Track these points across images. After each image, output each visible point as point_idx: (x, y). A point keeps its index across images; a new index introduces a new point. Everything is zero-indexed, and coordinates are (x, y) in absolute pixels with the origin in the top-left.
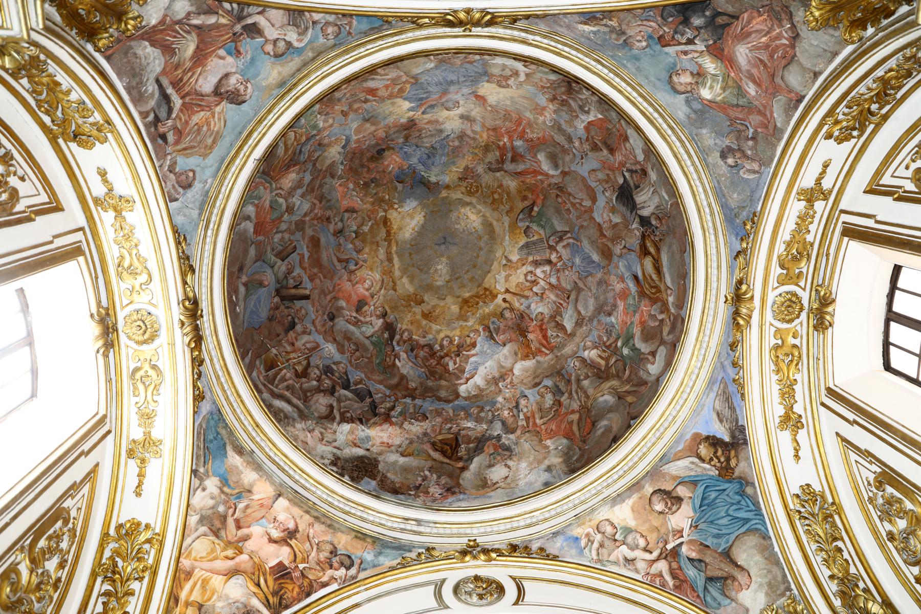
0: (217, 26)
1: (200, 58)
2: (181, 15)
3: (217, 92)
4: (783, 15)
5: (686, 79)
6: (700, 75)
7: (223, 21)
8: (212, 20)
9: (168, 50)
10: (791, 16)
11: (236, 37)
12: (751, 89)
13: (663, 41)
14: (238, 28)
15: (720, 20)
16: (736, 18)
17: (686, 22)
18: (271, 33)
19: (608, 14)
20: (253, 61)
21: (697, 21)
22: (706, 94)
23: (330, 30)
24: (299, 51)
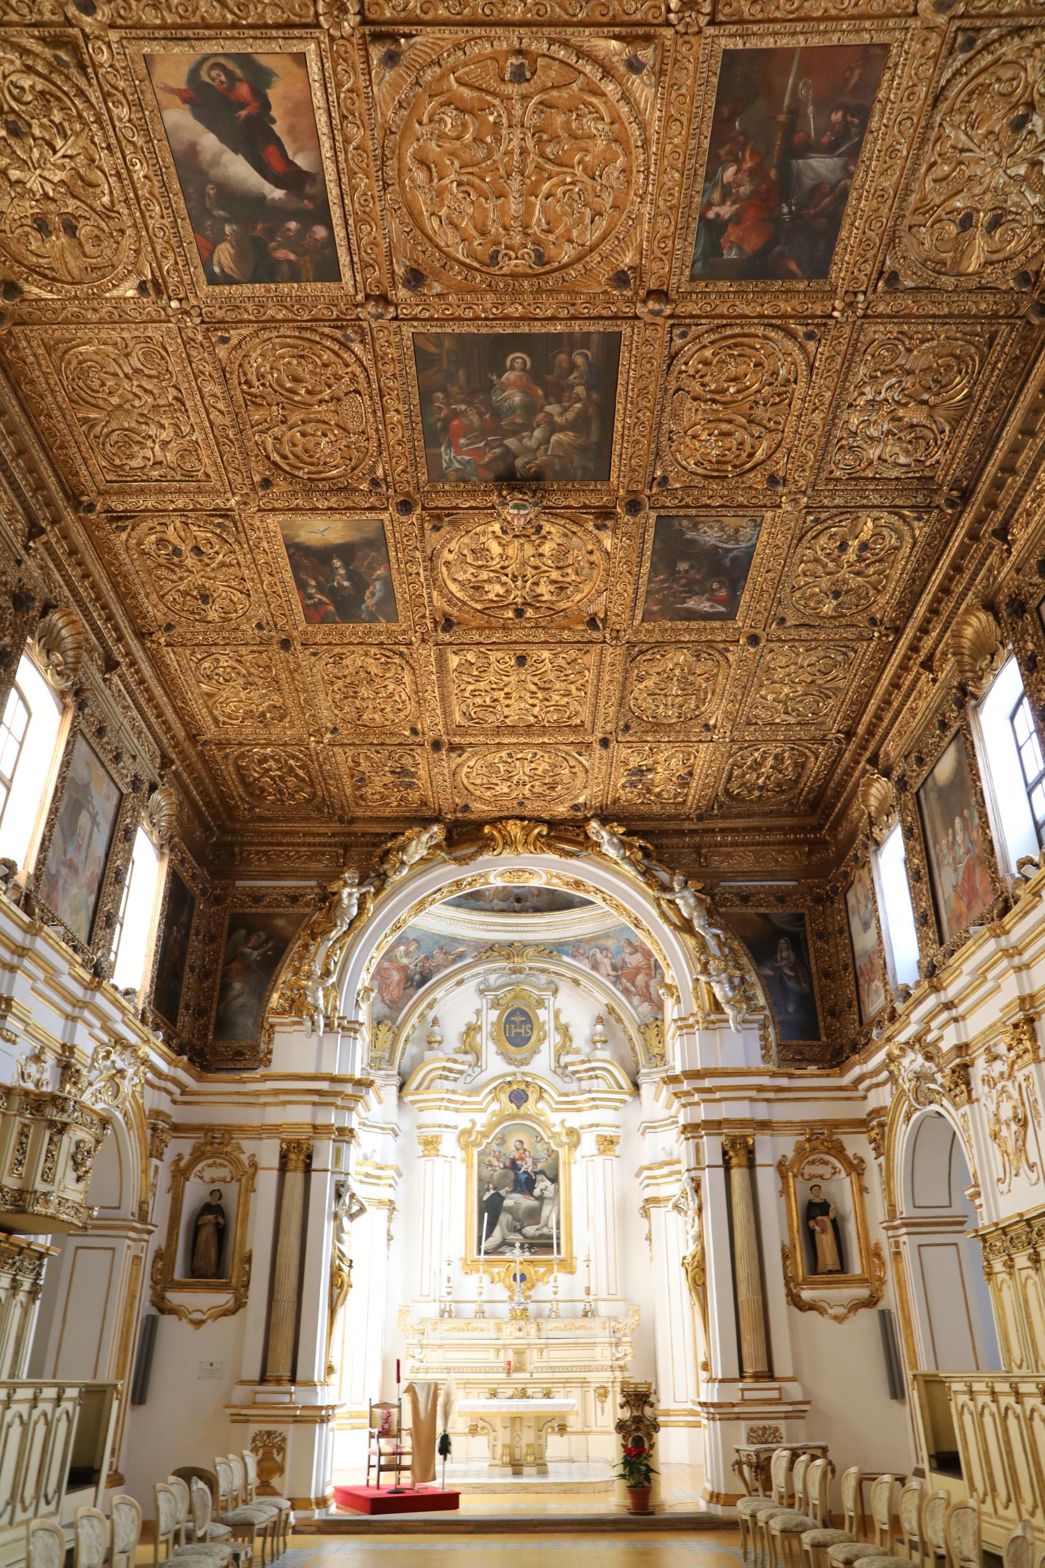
0: (629, 980)
1: (638, 970)
3: (636, 951)
5: (412, 948)
6: (407, 954)
7: (624, 980)
8: (628, 985)
9: (647, 986)
10: (390, 1008)
11: (622, 968)
12: (386, 965)
13: (427, 958)
17: (421, 973)
18: (607, 961)
19: (454, 961)
21: (417, 977)
22: (402, 948)
24: (597, 947)
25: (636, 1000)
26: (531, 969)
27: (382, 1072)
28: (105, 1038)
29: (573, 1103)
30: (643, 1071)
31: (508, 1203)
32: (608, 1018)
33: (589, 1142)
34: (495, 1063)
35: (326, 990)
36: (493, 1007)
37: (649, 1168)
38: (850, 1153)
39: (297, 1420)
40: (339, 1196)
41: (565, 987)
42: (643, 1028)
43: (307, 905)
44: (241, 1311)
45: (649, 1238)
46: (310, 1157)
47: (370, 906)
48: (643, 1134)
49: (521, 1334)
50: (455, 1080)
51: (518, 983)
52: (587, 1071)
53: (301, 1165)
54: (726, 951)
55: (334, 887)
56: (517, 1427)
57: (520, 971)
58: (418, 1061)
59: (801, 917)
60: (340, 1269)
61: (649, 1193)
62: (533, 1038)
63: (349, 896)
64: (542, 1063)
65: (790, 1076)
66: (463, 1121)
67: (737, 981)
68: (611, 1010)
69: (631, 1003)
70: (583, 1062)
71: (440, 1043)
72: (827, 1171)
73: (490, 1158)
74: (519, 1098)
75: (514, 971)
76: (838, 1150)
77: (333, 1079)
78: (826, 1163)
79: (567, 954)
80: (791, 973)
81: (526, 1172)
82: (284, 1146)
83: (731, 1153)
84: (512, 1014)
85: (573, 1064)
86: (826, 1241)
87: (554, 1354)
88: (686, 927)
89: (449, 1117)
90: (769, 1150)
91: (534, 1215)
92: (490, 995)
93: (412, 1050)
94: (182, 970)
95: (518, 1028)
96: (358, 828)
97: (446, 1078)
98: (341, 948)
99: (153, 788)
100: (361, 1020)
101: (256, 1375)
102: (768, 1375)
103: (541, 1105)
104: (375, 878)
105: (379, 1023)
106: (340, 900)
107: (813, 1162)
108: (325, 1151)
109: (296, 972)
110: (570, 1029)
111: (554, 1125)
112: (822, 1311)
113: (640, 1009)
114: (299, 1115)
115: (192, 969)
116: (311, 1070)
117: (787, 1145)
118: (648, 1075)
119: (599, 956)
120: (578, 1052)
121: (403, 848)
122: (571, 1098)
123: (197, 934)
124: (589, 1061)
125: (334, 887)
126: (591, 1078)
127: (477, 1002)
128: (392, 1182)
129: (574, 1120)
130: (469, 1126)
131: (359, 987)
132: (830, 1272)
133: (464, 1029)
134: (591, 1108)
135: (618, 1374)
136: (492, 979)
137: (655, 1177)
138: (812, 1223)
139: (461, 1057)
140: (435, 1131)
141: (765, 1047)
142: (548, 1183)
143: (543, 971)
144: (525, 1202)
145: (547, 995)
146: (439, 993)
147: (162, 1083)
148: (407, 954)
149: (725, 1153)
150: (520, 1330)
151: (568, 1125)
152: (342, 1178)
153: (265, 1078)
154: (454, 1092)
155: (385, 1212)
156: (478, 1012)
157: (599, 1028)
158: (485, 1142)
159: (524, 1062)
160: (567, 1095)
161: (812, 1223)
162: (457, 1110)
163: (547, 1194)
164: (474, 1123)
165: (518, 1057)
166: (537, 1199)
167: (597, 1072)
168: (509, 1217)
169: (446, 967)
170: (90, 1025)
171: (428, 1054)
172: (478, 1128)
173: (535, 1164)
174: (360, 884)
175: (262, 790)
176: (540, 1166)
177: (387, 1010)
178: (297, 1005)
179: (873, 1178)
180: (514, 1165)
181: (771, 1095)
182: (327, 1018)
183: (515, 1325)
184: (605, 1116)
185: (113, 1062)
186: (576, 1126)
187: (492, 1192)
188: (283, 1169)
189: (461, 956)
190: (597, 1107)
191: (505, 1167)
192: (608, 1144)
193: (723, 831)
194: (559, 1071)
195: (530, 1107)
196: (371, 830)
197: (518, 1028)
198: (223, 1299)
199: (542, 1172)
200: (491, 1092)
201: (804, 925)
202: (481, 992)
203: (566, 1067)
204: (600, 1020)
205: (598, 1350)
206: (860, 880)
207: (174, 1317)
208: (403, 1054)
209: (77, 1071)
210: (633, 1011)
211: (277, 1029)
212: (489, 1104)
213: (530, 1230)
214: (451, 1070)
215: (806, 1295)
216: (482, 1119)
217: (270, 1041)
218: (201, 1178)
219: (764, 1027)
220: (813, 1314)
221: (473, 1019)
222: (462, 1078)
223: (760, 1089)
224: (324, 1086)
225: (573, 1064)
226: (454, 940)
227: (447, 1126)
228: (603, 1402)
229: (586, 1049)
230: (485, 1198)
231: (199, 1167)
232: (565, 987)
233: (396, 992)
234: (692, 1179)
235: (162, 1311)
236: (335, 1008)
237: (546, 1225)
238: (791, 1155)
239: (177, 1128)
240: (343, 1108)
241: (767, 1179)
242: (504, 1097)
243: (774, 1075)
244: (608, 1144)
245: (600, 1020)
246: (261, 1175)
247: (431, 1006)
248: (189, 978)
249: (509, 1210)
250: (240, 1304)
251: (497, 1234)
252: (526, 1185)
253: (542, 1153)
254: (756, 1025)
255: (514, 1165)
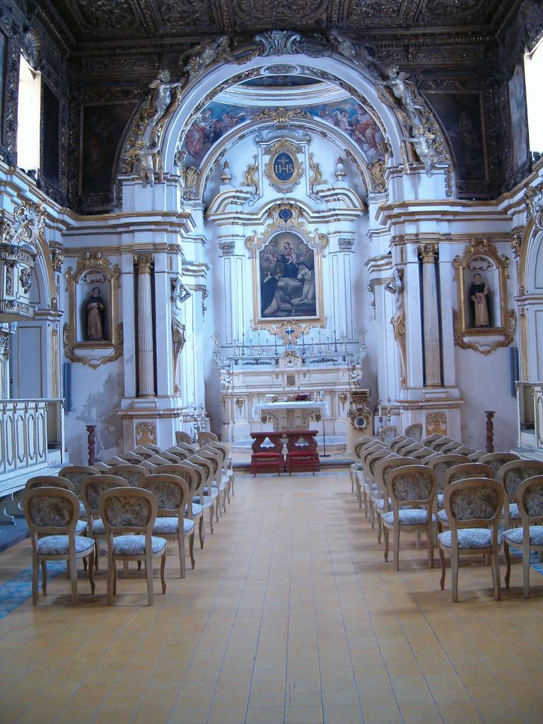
1: (367, 126)
2: (366, 145)
4: (194, 155)
9: (374, 138)
13: (218, 121)
14: (354, 127)
15: (207, 140)
16: (204, 144)
19: (237, 123)
20: (353, 114)
21: (212, 135)
23: (327, 113)
25: (366, 147)
26: (291, 126)
27: (192, 202)
28: (19, 201)
29: (322, 217)
30: (370, 195)
31: (281, 284)
32: (347, 161)
33: (334, 243)
34: (269, 194)
35: (154, 156)
36: (265, 153)
37: (374, 260)
38: (499, 254)
39: (160, 416)
40: (173, 288)
41: (316, 139)
42: (370, 166)
43: (135, 97)
44: (120, 358)
45: (374, 304)
46: (153, 264)
47: (179, 97)
48: (370, 237)
49: (289, 364)
50: (242, 204)
51: (283, 137)
52: (332, 195)
53: (148, 270)
54: (424, 121)
55: (152, 86)
56: (291, 417)
57: (284, 128)
58: (215, 192)
59: (477, 97)
60: (178, 331)
61: (374, 275)
62: (295, 174)
63: (164, 91)
64: (300, 192)
65: (464, 205)
66: (249, 232)
67: (431, 142)
68: (348, 153)
69: (362, 149)
70: (329, 190)
71: (230, 179)
72: (485, 264)
73: (268, 255)
74: (285, 215)
75: (280, 128)
76: (493, 253)
77: (164, 215)
78: (484, 260)
79: (317, 115)
80: (469, 136)
81: (292, 263)
82: (136, 258)
83: (424, 254)
84: (279, 157)
85: (323, 191)
86: (481, 308)
87: (314, 375)
88: (399, 103)
89: (239, 230)
90: (447, 252)
91: (298, 291)
92: (264, 145)
93: (211, 185)
94: (57, 148)
95: (284, 168)
96: (167, 41)
97: (236, 203)
98: (161, 127)
99: (26, 30)
100: (179, 174)
101: (134, 394)
102: (442, 385)
103: (300, 220)
104: (181, 76)
105: (187, 168)
106: (158, 92)
107: (476, 260)
108: (162, 260)
109: (133, 146)
110: (322, 168)
111: (310, 232)
112: (475, 349)
113: (369, 153)
114: (143, 238)
115: (63, 148)
116: (149, 209)
117: (459, 249)
118: (373, 198)
119: (339, 116)
120: (325, 182)
121: (199, 54)
122: (322, 214)
123: (64, 123)
124: (334, 189)
125: (152, 86)
126: (335, 200)
127: (254, 150)
128: (203, 273)
129: (323, 229)
130: (252, 234)
131: (176, 151)
132: (482, 326)
133: (246, 169)
134: (335, 220)
135: (353, 386)
136: (264, 133)
137: (378, 266)
138: (473, 298)
139: (245, 189)
140: (228, 240)
141: (449, 186)
142: (307, 270)
143: (300, 127)
144: (293, 283)
145: (303, 144)
146: (227, 146)
147: (55, 225)
148: (204, 119)
149: (420, 254)
150: (290, 362)
151: (319, 232)
152: (175, 276)
153: (119, 217)
154: (241, 213)
155: (201, 293)
156: (255, 157)
157: (340, 166)
158: (264, 245)
159: (289, 190)
160: (318, 212)
161: (473, 298)
162: (244, 225)
163: (306, 277)
164: (255, 232)
165: (285, 188)
166: (299, 281)
167: (339, 196)
168: (281, 292)
169: (232, 127)
170: (11, 195)
171: (223, 189)
172: (259, 236)
173: (298, 256)
174: (171, 82)
175: (98, 19)
176: (301, 259)
177: (192, 159)
178: (134, 165)
179: (513, 271)
180: (283, 259)
181: (451, 217)
182: (155, 174)
183: (288, 359)
184: (345, 226)
185: (26, 216)
186: (325, 233)
187: (270, 277)
188: (136, 273)
189: (242, 119)
190: (339, 220)
191: (278, 260)
192: (346, 244)
193: (424, 35)
194: (313, 196)
195: (295, 220)
196: (176, 42)
197: (284, 168)
198: (110, 352)
199: (303, 263)
200: (266, 212)
201: (478, 103)
202: (257, 143)
203: (318, 193)
204: (341, 160)
205: (341, 373)
206: (518, 73)
207: (81, 364)
208: (205, 188)
209: (8, 225)
210: (362, 155)
211: (123, 183)
212: (265, 220)
213: (296, 301)
214: (238, 198)
215: (466, 339)
216: (261, 229)
217: (120, 191)
218: (86, 281)
219: (448, 172)
220: (471, 351)
221: (252, 162)
222: (247, 202)
223: (444, 213)
224: (158, 219)
225: (323, 191)
226: (236, 108)
227: (237, 236)
228: (343, 403)
229: (331, 181)
230: (265, 281)
231: (83, 275)
232: (316, 139)
233: (198, 147)
234: (399, 271)
235: (73, 361)
236: (161, 168)
237: (306, 297)
238: (461, 255)
239: (68, 252)
240: (172, 232)
241: (446, 270)
242: (276, 215)
243: (453, 204)
244: (346, 244)
245: (341, 160)
246: (124, 276)
247: (222, 154)
248: (62, 155)
249: (282, 288)
250: (119, 353)
251: (274, 304)
252: (291, 271)
253: (304, 251)
254: (443, 171)
255: (283, 259)
